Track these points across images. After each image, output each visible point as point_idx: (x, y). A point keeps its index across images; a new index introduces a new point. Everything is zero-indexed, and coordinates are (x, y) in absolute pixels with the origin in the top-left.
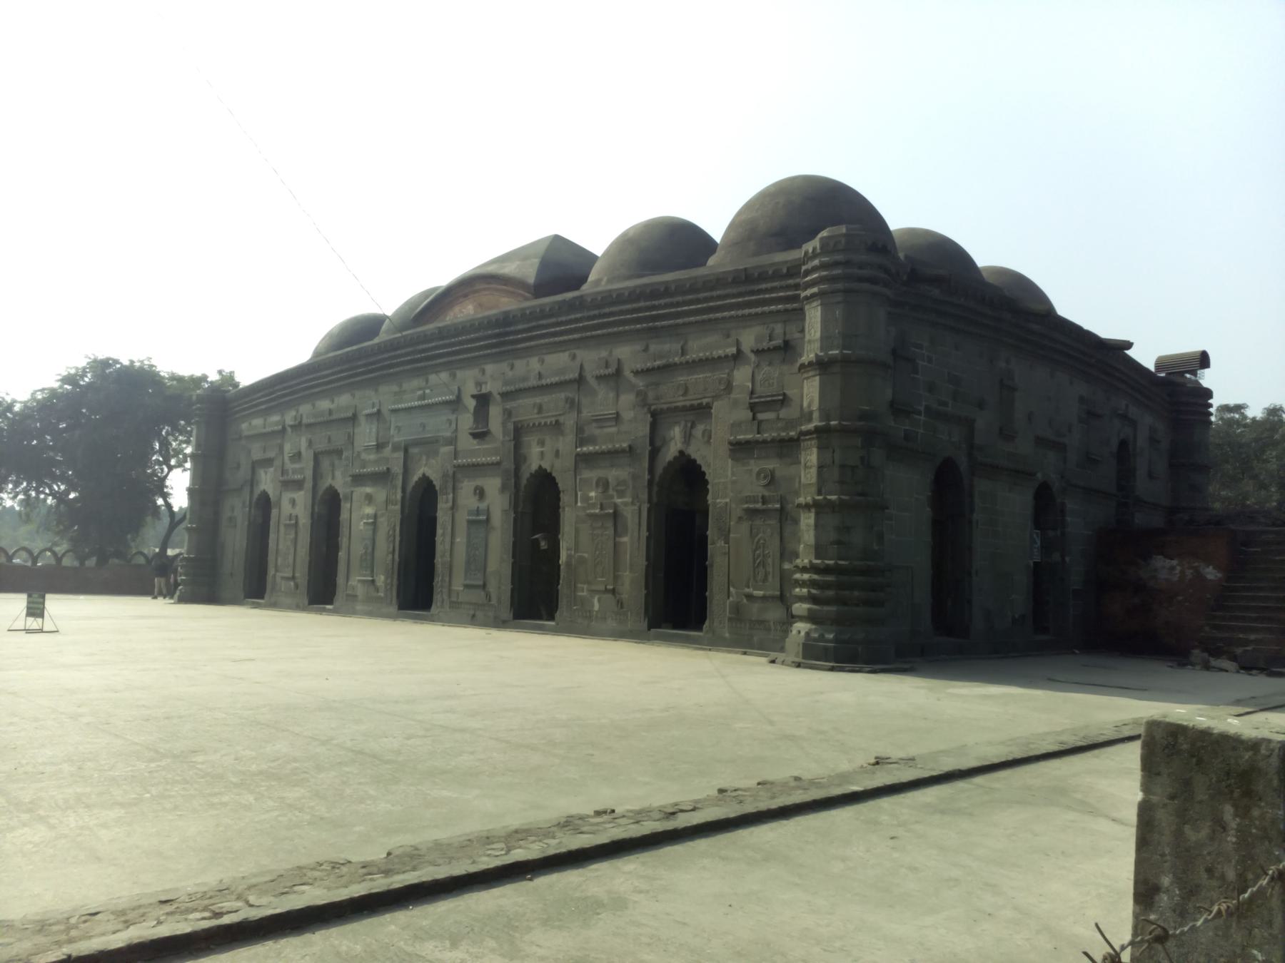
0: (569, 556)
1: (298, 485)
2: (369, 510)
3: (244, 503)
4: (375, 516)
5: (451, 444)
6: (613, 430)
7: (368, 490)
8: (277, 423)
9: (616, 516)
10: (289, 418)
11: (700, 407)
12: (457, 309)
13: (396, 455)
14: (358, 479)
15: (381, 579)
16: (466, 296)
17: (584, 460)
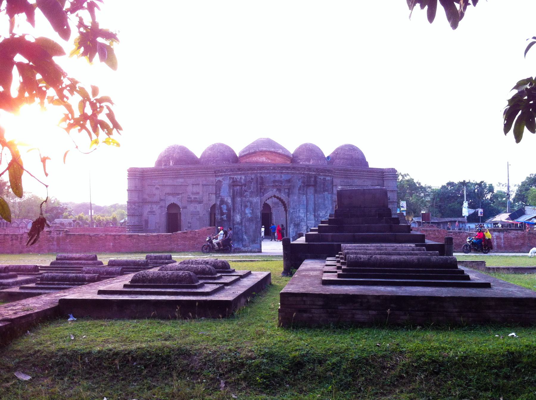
1: (200, 202)
3: (161, 207)
8: (182, 182)
10: (190, 181)
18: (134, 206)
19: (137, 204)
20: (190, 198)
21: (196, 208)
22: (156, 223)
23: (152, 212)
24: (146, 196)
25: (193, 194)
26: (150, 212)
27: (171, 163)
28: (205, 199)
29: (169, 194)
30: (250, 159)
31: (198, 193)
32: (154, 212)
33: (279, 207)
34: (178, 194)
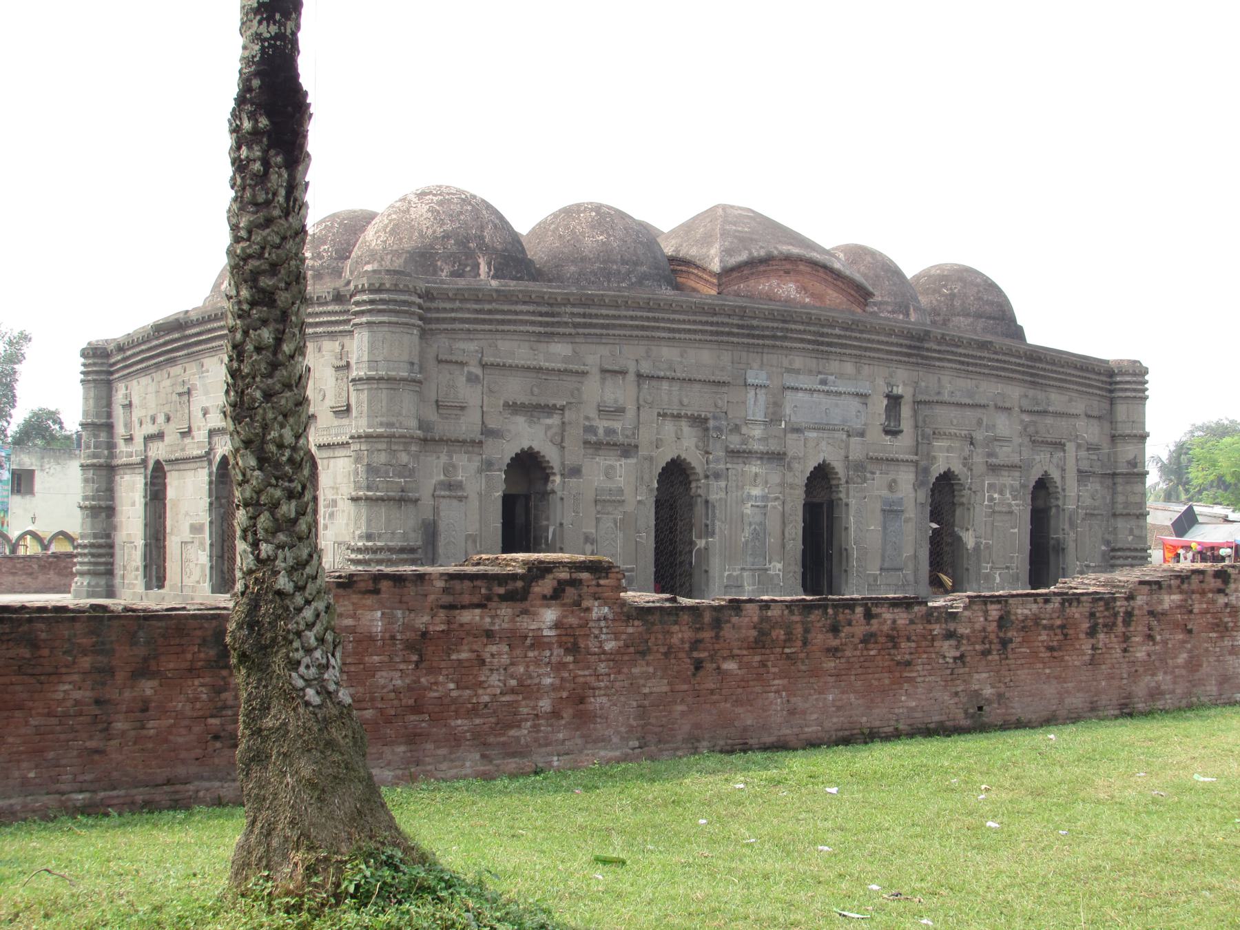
0: (978, 545)
1: (627, 450)
2: (756, 492)
3: (488, 465)
4: (765, 498)
5: (862, 434)
6: (1009, 449)
7: (754, 469)
8: (566, 359)
9: (1011, 513)
10: (594, 356)
11: (1060, 443)
12: (775, 282)
13: (795, 436)
14: (735, 454)
15: (776, 567)
16: (787, 272)
17: (994, 469)
18: (404, 458)
19: (414, 448)
20: (591, 429)
21: (609, 473)
22: (468, 537)
23: (452, 488)
24: (431, 415)
25: (603, 411)
26: (441, 483)
27: (483, 268)
28: (645, 437)
29: (514, 408)
30: (752, 283)
31: (620, 410)
32: (459, 486)
33: (865, 480)
34: (549, 410)
